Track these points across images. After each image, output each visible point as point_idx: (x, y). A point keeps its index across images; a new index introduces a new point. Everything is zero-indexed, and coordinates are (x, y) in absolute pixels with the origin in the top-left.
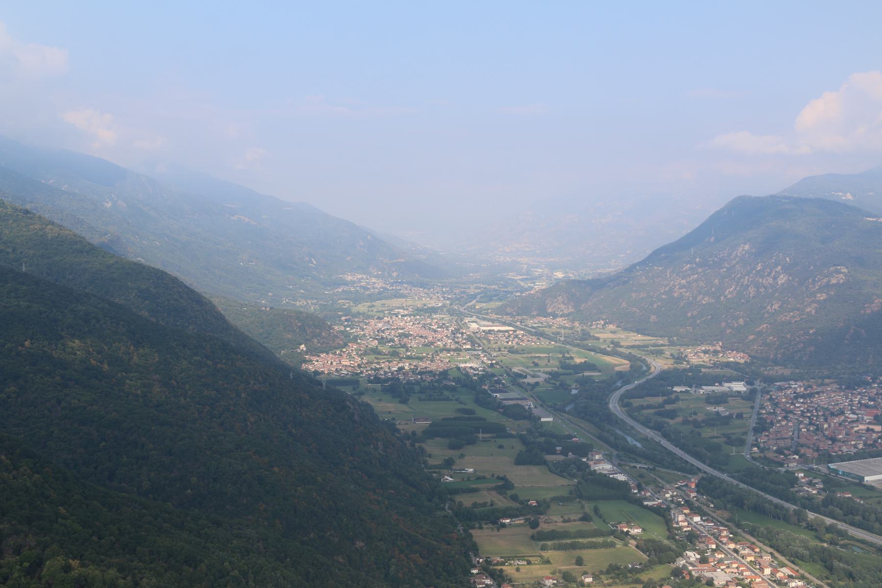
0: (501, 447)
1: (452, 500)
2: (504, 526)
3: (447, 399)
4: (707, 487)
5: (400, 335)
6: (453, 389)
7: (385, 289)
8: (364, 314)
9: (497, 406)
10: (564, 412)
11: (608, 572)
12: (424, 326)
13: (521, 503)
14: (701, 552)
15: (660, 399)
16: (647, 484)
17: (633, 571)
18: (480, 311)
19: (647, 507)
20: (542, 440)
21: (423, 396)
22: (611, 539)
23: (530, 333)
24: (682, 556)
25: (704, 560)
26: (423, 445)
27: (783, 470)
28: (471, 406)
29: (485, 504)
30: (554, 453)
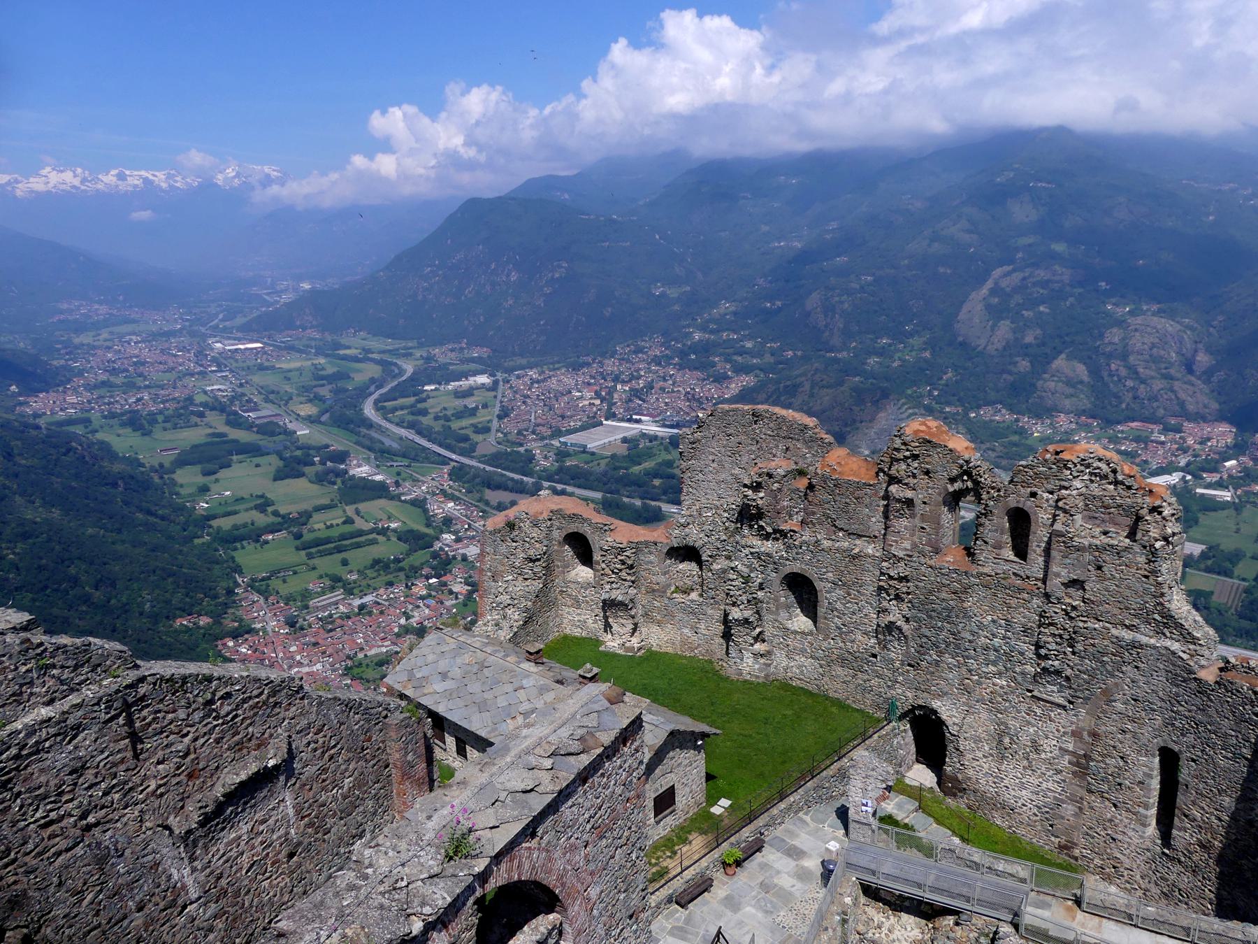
0: (257, 466)
1: (210, 527)
2: (267, 542)
3: (196, 425)
4: (458, 474)
5: (135, 364)
6: (201, 415)
7: (111, 314)
8: (88, 345)
9: (249, 426)
10: (320, 423)
11: (372, 566)
12: (162, 351)
13: (283, 517)
14: (455, 533)
15: (413, 399)
16: (404, 480)
17: (397, 560)
18: (225, 329)
19: (405, 501)
20: (298, 453)
21: (168, 425)
22: (374, 535)
23: (279, 348)
24: (438, 539)
25: (458, 540)
26: (173, 476)
27: (522, 449)
28: (223, 429)
29: (245, 525)
30: (313, 464)
